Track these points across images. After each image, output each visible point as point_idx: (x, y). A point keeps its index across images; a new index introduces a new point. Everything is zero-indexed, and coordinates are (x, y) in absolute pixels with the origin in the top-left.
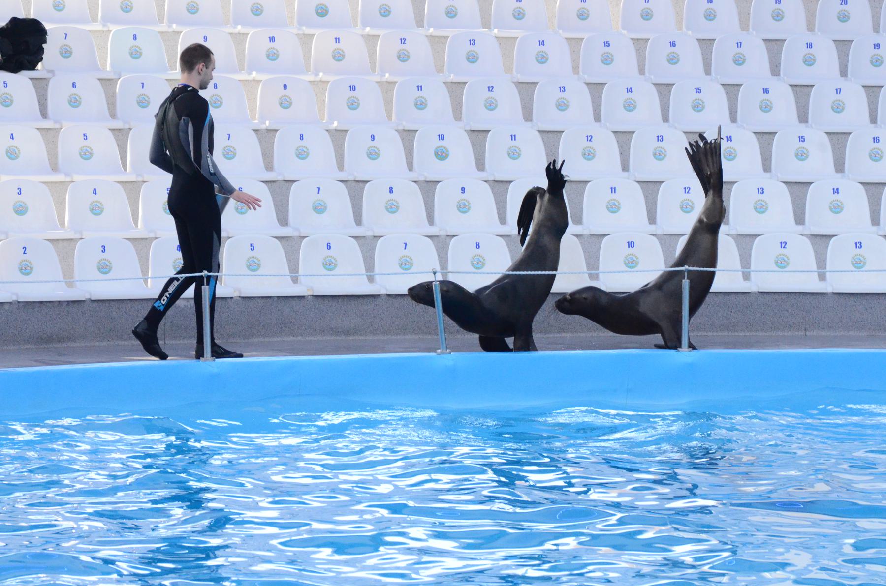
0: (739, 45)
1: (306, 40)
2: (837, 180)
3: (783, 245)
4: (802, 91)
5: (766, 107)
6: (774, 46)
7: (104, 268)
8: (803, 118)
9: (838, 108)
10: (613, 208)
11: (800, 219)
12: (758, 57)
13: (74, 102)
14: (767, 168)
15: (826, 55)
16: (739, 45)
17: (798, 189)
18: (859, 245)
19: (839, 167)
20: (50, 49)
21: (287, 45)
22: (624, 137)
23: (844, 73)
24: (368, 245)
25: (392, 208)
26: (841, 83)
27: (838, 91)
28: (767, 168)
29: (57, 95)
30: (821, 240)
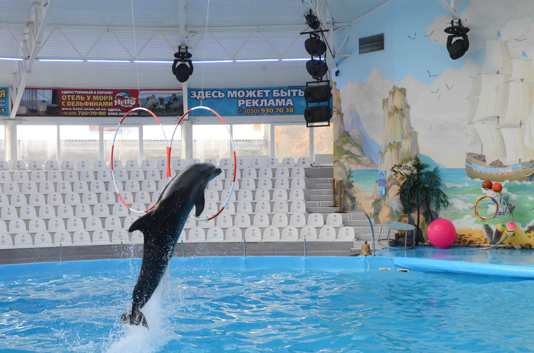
0: (11, 185)
3: (23, 236)
4: (28, 196)
5: (18, 201)
6: (20, 185)
11: (28, 229)
12: (16, 188)
14: (19, 216)
15: (34, 187)
16: (11, 185)
17: (27, 221)
18: (43, 235)
19: (38, 215)
23: (39, 191)
26: (38, 194)
27: (37, 196)
28: (19, 216)
30: (33, 235)
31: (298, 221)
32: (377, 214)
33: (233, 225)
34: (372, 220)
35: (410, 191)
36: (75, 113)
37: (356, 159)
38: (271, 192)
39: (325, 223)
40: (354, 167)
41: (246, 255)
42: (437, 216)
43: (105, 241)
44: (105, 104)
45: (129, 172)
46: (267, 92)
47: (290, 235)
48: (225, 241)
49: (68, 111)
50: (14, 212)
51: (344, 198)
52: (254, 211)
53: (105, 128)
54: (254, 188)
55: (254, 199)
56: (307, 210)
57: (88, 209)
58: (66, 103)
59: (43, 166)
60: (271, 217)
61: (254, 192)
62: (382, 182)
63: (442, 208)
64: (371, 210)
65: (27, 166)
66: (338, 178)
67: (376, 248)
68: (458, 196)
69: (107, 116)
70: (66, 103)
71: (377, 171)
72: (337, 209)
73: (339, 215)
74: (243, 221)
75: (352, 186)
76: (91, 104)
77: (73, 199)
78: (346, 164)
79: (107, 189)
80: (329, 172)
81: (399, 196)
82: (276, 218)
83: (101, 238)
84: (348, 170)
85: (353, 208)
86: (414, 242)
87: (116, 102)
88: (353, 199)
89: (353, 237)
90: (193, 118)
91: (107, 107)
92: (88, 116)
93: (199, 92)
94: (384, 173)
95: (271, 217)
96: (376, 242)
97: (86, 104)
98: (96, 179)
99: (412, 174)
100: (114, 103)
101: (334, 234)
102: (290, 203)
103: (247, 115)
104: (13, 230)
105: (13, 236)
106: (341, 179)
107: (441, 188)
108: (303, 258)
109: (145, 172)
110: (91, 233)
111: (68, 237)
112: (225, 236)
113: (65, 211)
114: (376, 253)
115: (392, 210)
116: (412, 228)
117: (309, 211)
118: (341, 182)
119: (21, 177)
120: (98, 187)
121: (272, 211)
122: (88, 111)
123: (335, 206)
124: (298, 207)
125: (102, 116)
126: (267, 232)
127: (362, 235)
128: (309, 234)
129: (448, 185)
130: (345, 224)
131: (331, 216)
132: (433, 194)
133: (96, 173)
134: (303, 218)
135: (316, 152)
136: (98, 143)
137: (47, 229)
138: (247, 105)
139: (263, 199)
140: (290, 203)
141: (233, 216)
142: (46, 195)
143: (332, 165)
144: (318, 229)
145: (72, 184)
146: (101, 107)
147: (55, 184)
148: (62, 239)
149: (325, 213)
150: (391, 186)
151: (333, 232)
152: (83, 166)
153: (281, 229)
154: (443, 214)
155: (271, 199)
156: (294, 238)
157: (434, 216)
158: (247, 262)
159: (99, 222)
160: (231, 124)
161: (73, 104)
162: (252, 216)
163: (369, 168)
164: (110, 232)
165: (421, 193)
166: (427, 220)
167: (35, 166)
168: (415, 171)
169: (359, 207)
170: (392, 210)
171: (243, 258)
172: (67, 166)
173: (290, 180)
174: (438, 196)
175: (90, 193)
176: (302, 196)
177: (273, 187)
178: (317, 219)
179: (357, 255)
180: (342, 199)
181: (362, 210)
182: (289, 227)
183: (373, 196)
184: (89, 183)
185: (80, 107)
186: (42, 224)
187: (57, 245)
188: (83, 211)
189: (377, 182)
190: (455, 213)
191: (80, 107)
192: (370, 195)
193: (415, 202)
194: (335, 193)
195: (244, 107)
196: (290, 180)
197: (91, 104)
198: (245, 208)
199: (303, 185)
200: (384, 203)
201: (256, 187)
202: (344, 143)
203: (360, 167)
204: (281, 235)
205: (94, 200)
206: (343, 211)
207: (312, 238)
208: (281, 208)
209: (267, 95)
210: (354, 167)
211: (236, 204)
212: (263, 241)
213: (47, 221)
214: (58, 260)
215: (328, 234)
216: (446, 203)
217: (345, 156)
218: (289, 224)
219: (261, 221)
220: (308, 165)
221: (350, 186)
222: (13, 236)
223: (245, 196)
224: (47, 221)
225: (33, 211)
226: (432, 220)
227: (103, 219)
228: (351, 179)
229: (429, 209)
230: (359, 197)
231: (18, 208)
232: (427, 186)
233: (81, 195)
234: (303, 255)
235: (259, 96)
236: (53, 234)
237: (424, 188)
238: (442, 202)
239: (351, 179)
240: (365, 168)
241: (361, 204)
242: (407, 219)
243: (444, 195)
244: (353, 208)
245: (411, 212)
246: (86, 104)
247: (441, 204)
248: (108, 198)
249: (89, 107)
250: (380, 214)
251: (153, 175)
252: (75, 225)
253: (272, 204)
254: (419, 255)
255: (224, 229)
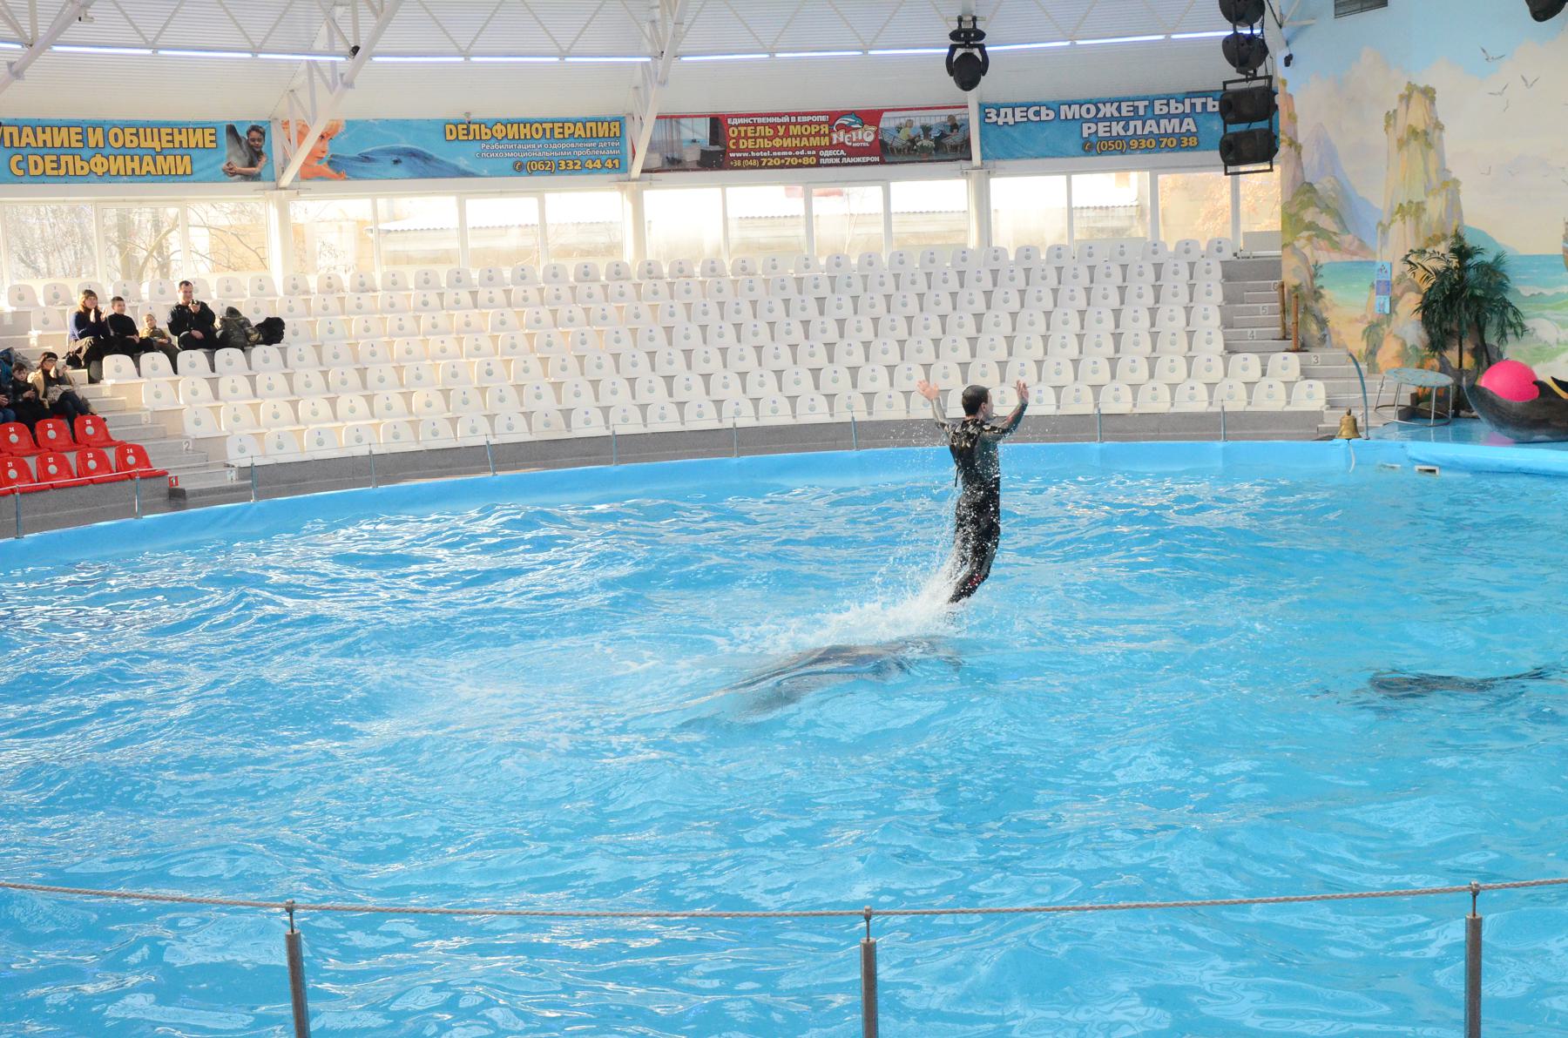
1: (417, 319)
2: (688, 374)
4: (669, 330)
5: (651, 339)
6: (654, 308)
7: (320, 443)
8: (670, 343)
9: (687, 337)
10: (577, 395)
11: (671, 395)
13: (301, 359)
14: (653, 370)
17: (669, 379)
19: (689, 367)
20: (287, 332)
21: (409, 324)
22: (581, 359)
24: (453, 421)
25: (465, 402)
29: (292, 355)
31: (1209, 370)
32: (1372, 352)
33: (1076, 379)
34: (1363, 366)
35: (1444, 305)
36: (755, 163)
37: (1330, 239)
38: (1153, 312)
39: (1264, 374)
40: (1324, 257)
41: (1103, 439)
42: (1500, 355)
43: (821, 416)
44: (815, 142)
45: (865, 277)
46: (1141, 105)
47: (1192, 398)
48: (1059, 412)
49: (742, 158)
50: (643, 360)
51: (1304, 322)
52: (1117, 350)
53: (815, 191)
54: (1117, 305)
55: (1117, 326)
56: (1226, 347)
57: (786, 352)
58: (736, 144)
59: (697, 270)
60: (1152, 362)
61: (1117, 313)
62: (1384, 287)
63: (1509, 337)
64: (1360, 346)
65: (666, 270)
66: (1291, 279)
67: (1371, 423)
68: (1546, 312)
69: (818, 165)
70: (736, 144)
71: (1374, 263)
72: (1290, 344)
73: (1294, 358)
74: (1095, 372)
75: (1321, 296)
76: (787, 142)
77: (755, 334)
78: (1307, 251)
79: (822, 313)
80: (1271, 268)
81: (1420, 315)
82: (1163, 365)
83: (812, 409)
84: (1312, 262)
85: (1323, 340)
86: (1451, 411)
87: (835, 136)
88: (1322, 323)
89: (1323, 402)
90: (990, 163)
91: (818, 148)
92: (782, 167)
93: (1003, 111)
94: (1388, 267)
95: (1152, 362)
96: (1370, 412)
97: (777, 143)
98: (800, 292)
99: (1448, 269)
100: (831, 139)
101: (1284, 397)
102: (1190, 334)
103: (1101, 153)
104: (643, 397)
105: (643, 408)
106: (1296, 282)
107: (1509, 297)
108: (1220, 444)
109: (897, 276)
110: (793, 399)
111: (748, 409)
112: (1058, 400)
113: (742, 358)
114: (1371, 433)
115: (1404, 344)
116: (1446, 380)
117: (1230, 350)
118: (1297, 288)
119: (655, 293)
120: (803, 309)
121: (1154, 350)
122: (782, 157)
123: (1284, 338)
124: (1209, 342)
125: (810, 166)
126: (1145, 393)
127: (1344, 397)
128: (1231, 397)
129: (1525, 291)
130: (1306, 374)
131: (1277, 359)
132: (1492, 311)
133: (799, 280)
134: (1218, 363)
135: (1245, 227)
136: (802, 220)
137: (708, 393)
138: (1101, 134)
139: (1137, 325)
140: (1190, 334)
141: (1076, 362)
142: (703, 328)
143: (1279, 252)
144: (1250, 385)
145: (754, 303)
146: (806, 148)
147: (721, 304)
148: (738, 413)
149: (1264, 353)
150: (1402, 294)
151: (1280, 390)
152: (774, 267)
153: (1173, 387)
154: (1513, 351)
155: (1153, 325)
156: (1200, 406)
157: (1494, 356)
158: (1103, 454)
159: (807, 379)
160: (1069, 173)
161: (750, 144)
162: (1113, 362)
163: (1356, 258)
164: (830, 397)
165: (1467, 308)
166: (1479, 363)
167: (681, 271)
168: (1454, 263)
169: (1335, 340)
170: (1404, 344)
171: (1097, 445)
172: (744, 269)
173: (1192, 287)
174: (1503, 314)
175: (788, 320)
176: (1215, 318)
177: (1157, 301)
178: (1250, 363)
179: (1331, 438)
180: (1299, 323)
181: (1344, 346)
182: (1190, 383)
183: (1365, 316)
184: (786, 301)
185: (765, 150)
186: (698, 384)
187: (728, 424)
188: (777, 357)
189: (1372, 286)
190: (1538, 349)
191: (765, 150)
192: (1359, 313)
193: (1454, 326)
194: (1284, 311)
195: (1093, 139)
196: (1192, 287)
197: (787, 142)
198: (1099, 345)
199: (1218, 295)
200: (1387, 331)
201: (1122, 302)
202: (1304, 206)
203: (1336, 257)
204: (1173, 398)
205: (797, 334)
206: (1300, 348)
207: (1238, 404)
208: (1173, 343)
209: (1141, 112)
210: (1324, 257)
211: (1080, 337)
212: (1136, 411)
213: (706, 377)
214: (730, 454)
215: (1270, 396)
216: (1520, 329)
217: (1306, 234)
218: (1189, 376)
219: (1133, 370)
220: (1227, 255)
221: (1317, 295)
222: (643, 408)
223: (1099, 321)
224: (706, 377)
225: (680, 360)
226: (1489, 364)
227: (816, 372)
228: (1318, 282)
229: (1482, 340)
230: (1335, 318)
231: (652, 354)
232: (1478, 292)
233: (771, 324)
234: (1217, 438)
235: (1124, 113)
236: (718, 403)
237: (1473, 297)
238: (1511, 325)
239: (1318, 282)
240: (1347, 258)
241: (1339, 334)
242: (1436, 362)
243: (1516, 313)
244: (1323, 340)
245: (1445, 348)
246: (777, 143)
247: (1509, 331)
248: (824, 331)
249: (782, 149)
250: (1379, 353)
251: (913, 283)
252: (762, 385)
253: (1154, 336)
254: (1461, 438)
255: (1058, 389)
